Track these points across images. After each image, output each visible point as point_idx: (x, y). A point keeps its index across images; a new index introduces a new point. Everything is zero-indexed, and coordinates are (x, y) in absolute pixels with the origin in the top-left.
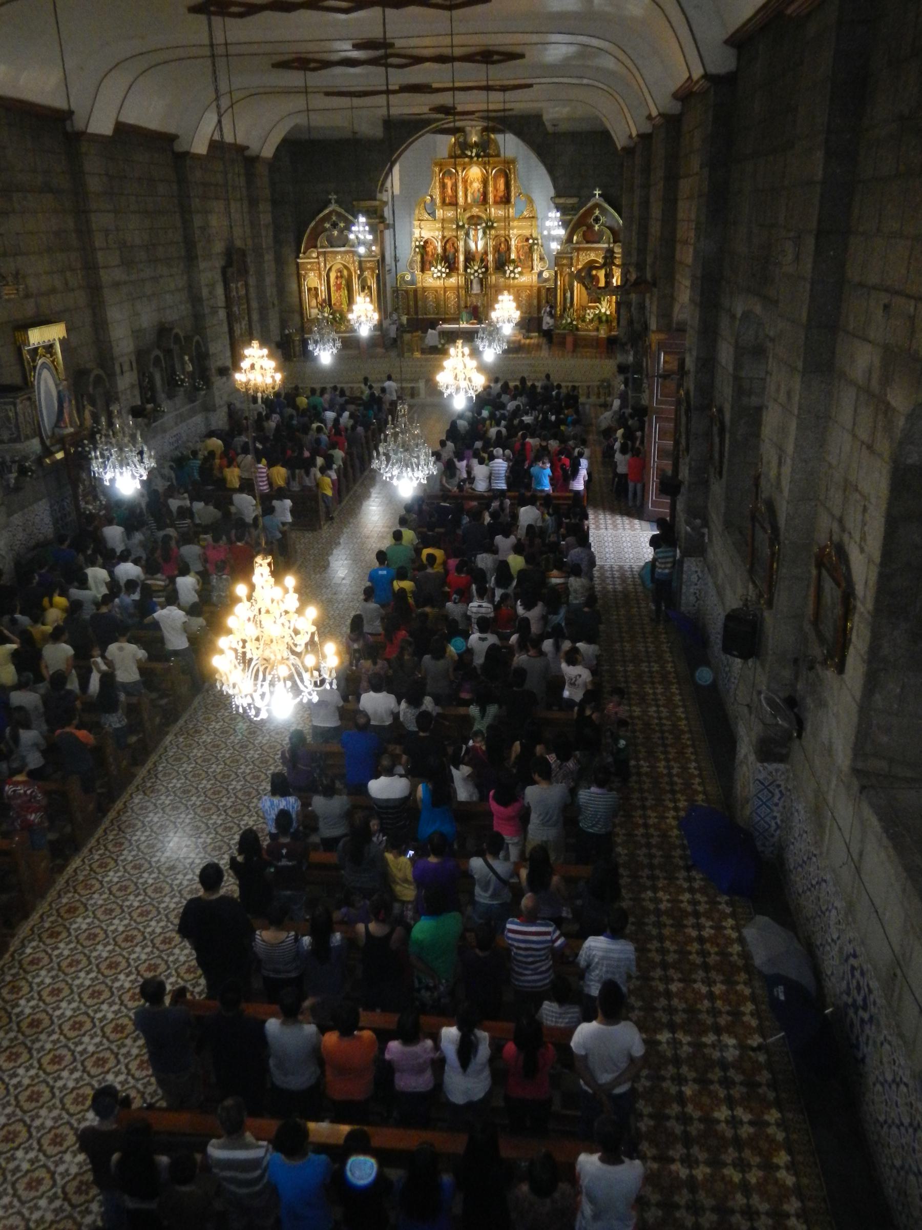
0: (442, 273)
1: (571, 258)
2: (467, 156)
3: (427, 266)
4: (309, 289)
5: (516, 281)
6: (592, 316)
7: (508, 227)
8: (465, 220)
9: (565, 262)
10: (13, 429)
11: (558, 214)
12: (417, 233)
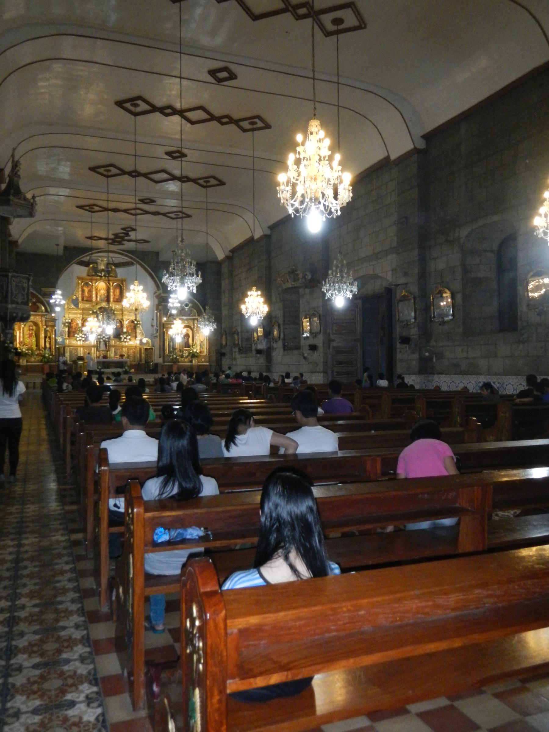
0: (82, 337)
3: (72, 334)
5: (127, 344)
6: (187, 354)
8: (97, 310)
10: (25, 296)
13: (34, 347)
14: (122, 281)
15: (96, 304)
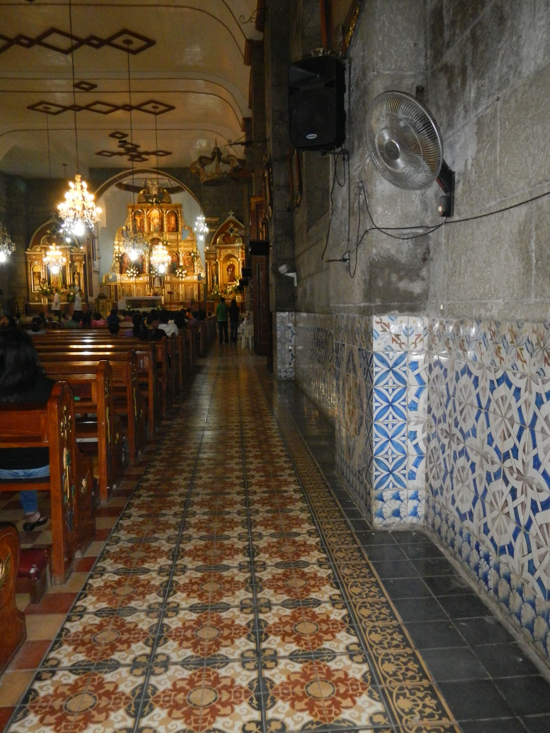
0: (134, 274)
1: (216, 254)
2: (150, 202)
3: (124, 270)
4: (34, 273)
7: (178, 246)
9: (212, 256)
11: (204, 218)
12: (117, 247)
13: (60, 285)
14: (176, 207)
15: (149, 234)
